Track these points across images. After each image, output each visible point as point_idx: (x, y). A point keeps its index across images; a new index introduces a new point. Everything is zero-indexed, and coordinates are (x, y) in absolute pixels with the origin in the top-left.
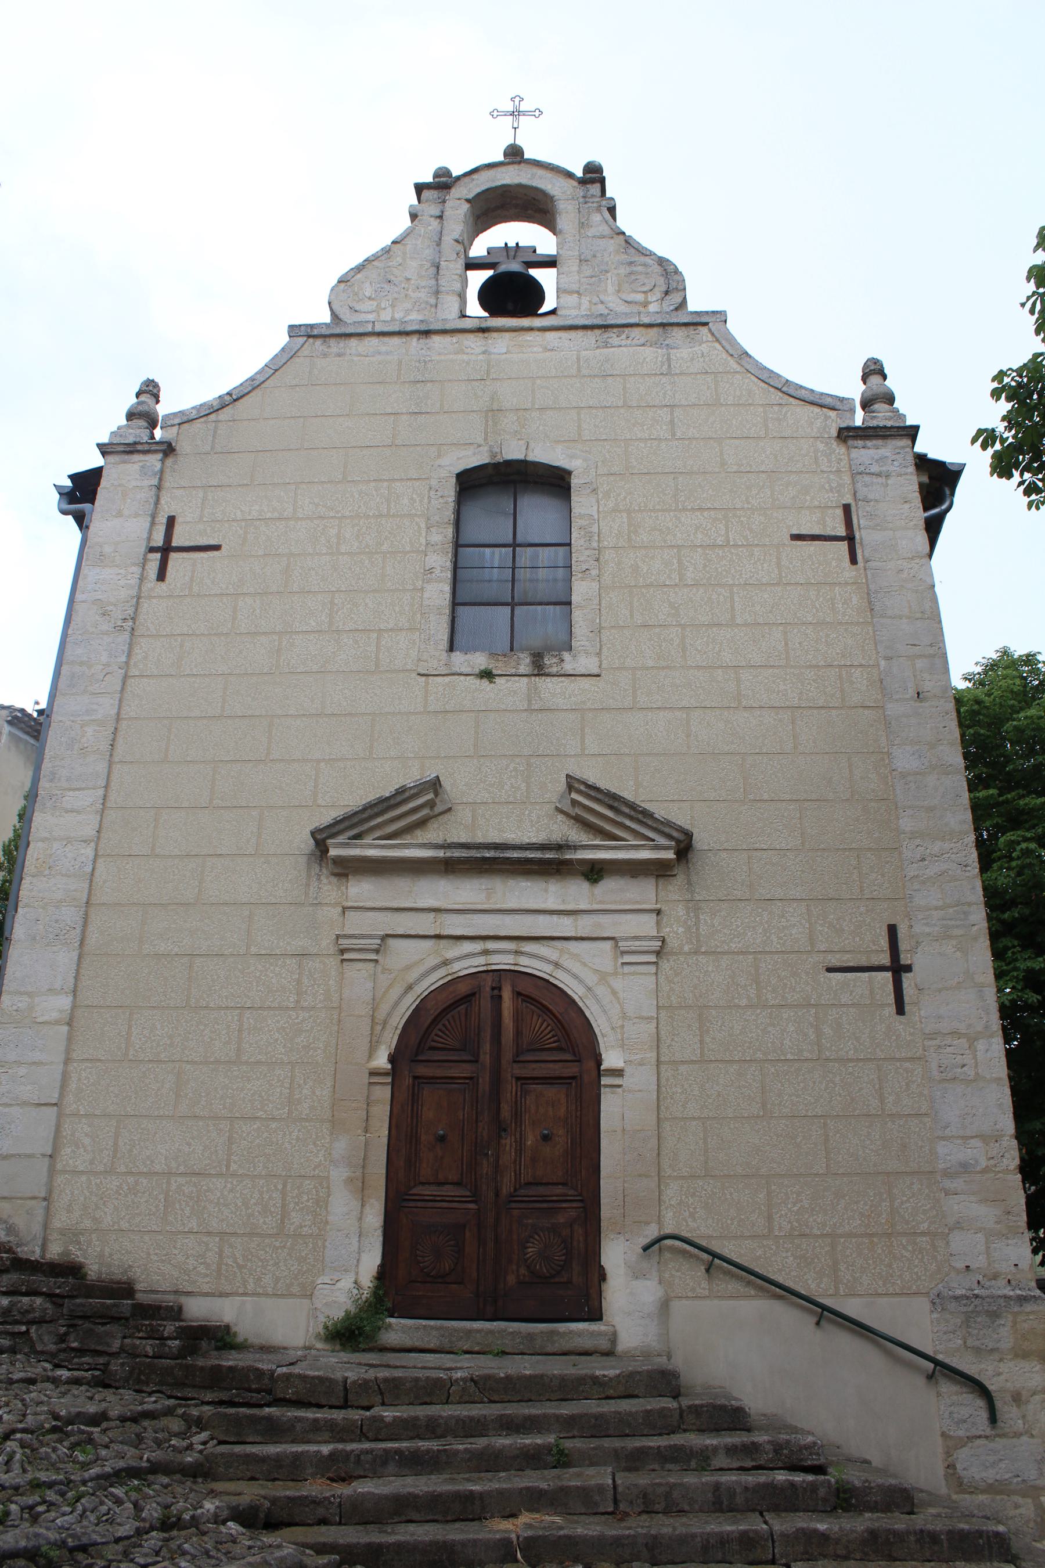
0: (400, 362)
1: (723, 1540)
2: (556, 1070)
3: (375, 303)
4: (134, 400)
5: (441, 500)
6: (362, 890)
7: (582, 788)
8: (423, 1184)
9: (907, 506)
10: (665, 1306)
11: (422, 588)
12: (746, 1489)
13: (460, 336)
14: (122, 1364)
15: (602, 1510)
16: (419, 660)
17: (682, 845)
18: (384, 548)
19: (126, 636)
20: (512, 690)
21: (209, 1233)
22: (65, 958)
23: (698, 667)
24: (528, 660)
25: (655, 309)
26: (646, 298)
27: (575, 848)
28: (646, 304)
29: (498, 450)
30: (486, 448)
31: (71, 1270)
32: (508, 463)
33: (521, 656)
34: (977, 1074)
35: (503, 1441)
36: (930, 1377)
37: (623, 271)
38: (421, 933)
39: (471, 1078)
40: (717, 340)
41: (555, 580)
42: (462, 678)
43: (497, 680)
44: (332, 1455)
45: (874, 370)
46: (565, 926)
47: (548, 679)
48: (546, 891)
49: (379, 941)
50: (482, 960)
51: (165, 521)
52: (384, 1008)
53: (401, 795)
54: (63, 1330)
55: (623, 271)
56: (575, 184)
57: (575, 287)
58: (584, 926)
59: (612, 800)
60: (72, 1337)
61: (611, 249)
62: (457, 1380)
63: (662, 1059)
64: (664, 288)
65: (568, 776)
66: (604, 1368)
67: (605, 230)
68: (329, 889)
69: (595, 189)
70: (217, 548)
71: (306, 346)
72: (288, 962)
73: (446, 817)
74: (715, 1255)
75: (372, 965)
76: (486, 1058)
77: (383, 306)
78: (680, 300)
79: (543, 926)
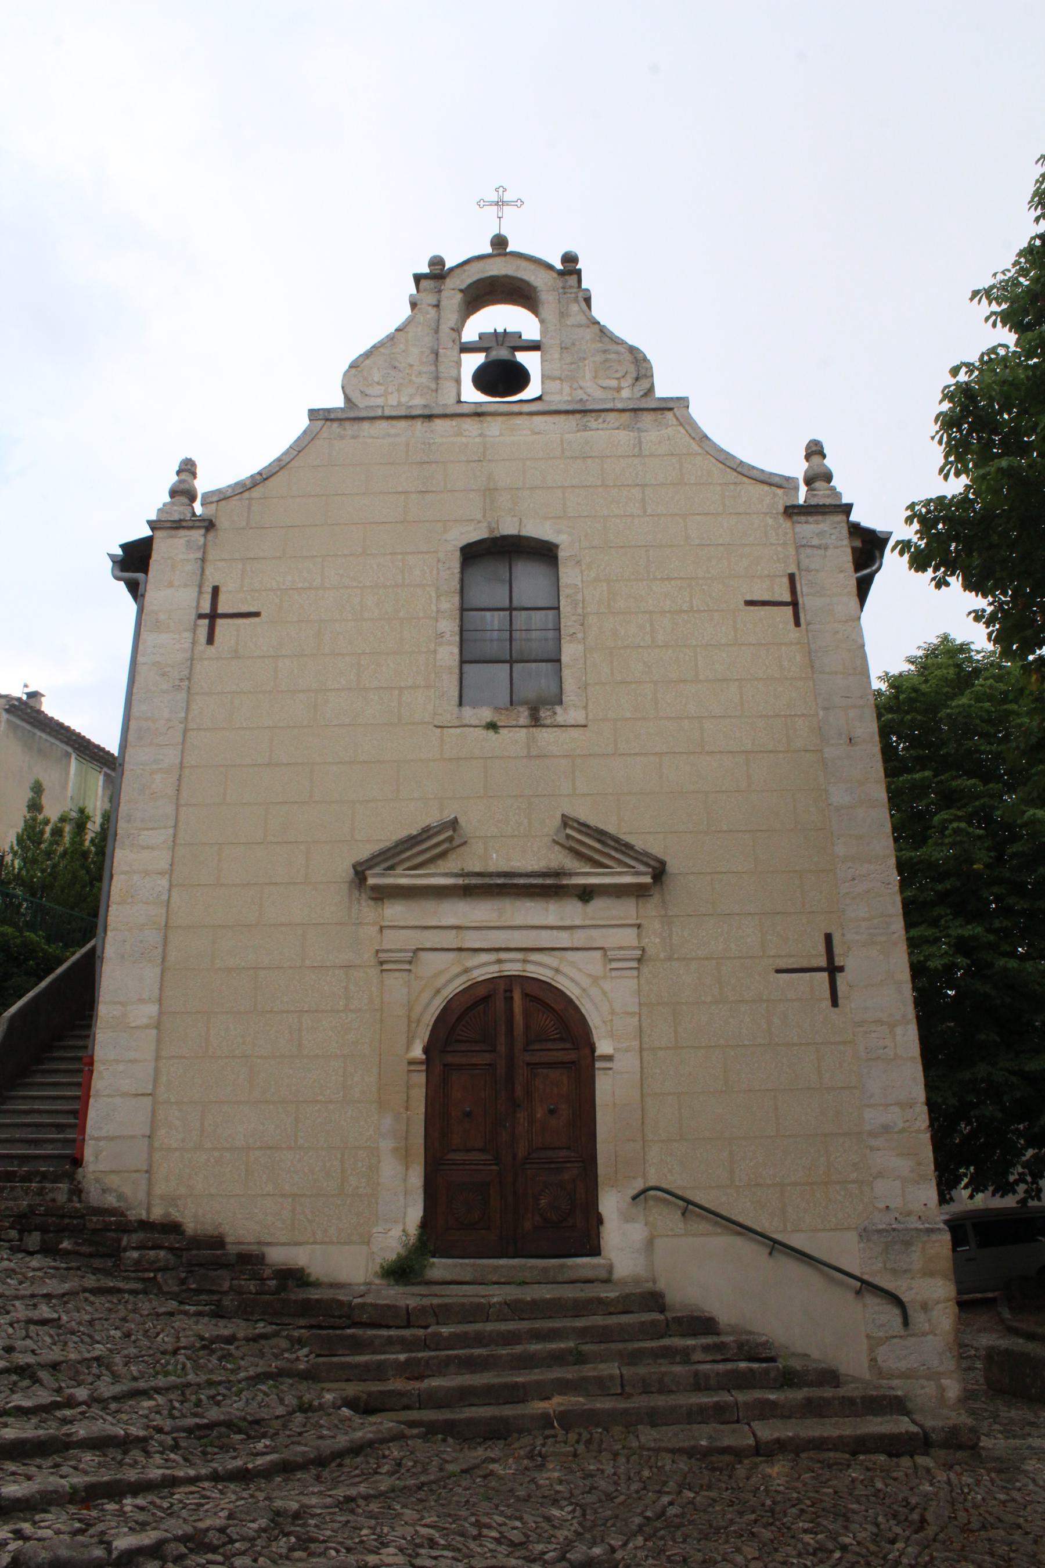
0: (408, 445)
1: (702, 1409)
2: (560, 1056)
3: (383, 388)
4: (175, 478)
5: (448, 572)
6: (395, 911)
7: (575, 825)
8: (455, 1151)
9: (842, 575)
10: (650, 1244)
11: (435, 651)
12: (718, 1374)
13: (459, 419)
14: (232, 1300)
15: (612, 1392)
16: (435, 714)
17: (658, 871)
18: (401, 614)
19: (183, 695)
20: (514, 739)
21: (283, 1196)
22: (151, 974)
23: (668, 718)
24: (526, 713)
25: (627, 394)
26: (619, 383)
27: (571, 875)
28: (619, 389)
29: (495, 526)
30: (485, 524)
31: (173, 1228)
32: (505, 538)
33: (521, 709)
34: (896, 1054)
35: (535, 1347)
36: (858, 1292)
37: (598, 358)
38: (446, 946)
39: (490, 1065)
40: (681, 424)
41: (546, 639)
42: (472, 729)
43: (502, 731)
44: (407, 1360)
45: (815, 451)
46: (563, 939)
47: (544, 730)
48: (547, 910)
49: (411, 954)
50: (495, 968)
51: (210, 590)
52: (417, 1010)
53: (427, 833)
54: (183, 1275)
55: (598, 358)
56: (555, 275)
57: (557, 373)
58: (579, 938)
59: (600, 835)
60: (191, 1280)
61: (588, 337)
62: (494, 1304)
63: (645, 1046)
64: (634, 375)
65: (563, 815)
66: (606, 1292)
67: (581, 319)
68: (368, 910)
69: (572, 280)
70: (257, 614)
71: (324, 429)
72: (337, 972)
73: (463, 848)
74: (689, 1202)
75: (405, 974)
76: (502, 1048)
77: (390, 390)
78: (648, 386)
79: (546, 939)
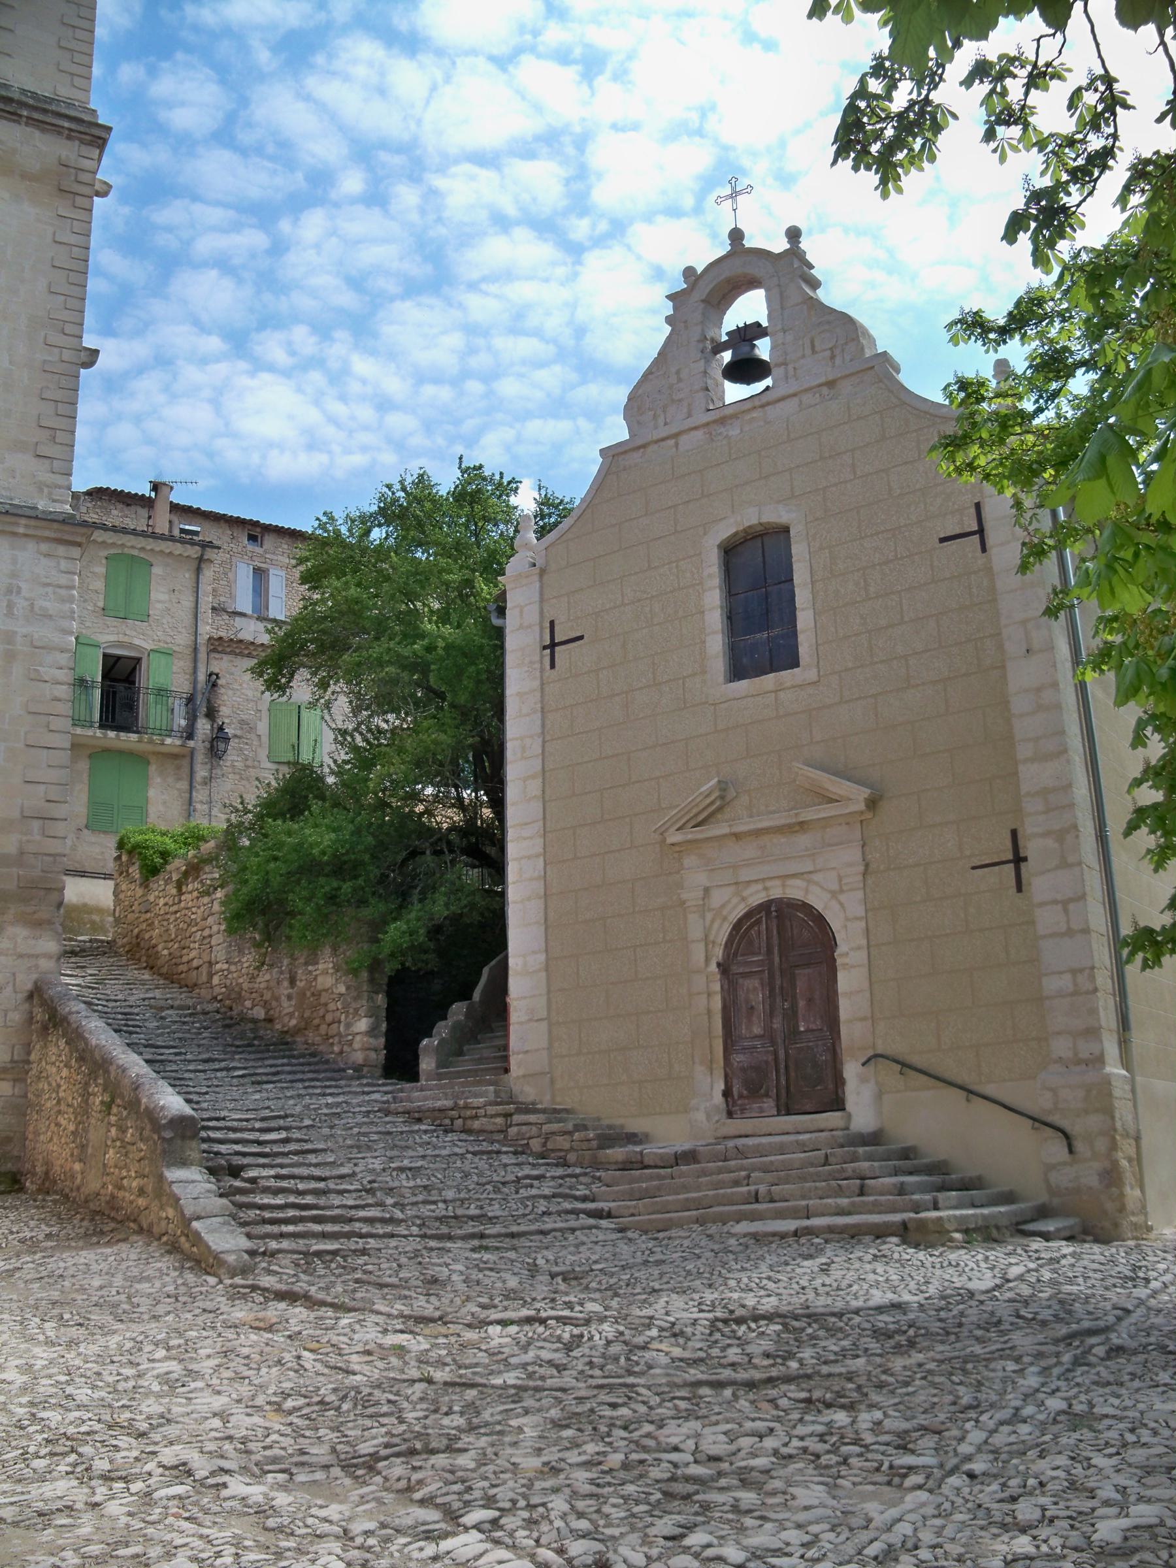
70: (581, 638)
